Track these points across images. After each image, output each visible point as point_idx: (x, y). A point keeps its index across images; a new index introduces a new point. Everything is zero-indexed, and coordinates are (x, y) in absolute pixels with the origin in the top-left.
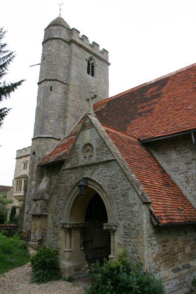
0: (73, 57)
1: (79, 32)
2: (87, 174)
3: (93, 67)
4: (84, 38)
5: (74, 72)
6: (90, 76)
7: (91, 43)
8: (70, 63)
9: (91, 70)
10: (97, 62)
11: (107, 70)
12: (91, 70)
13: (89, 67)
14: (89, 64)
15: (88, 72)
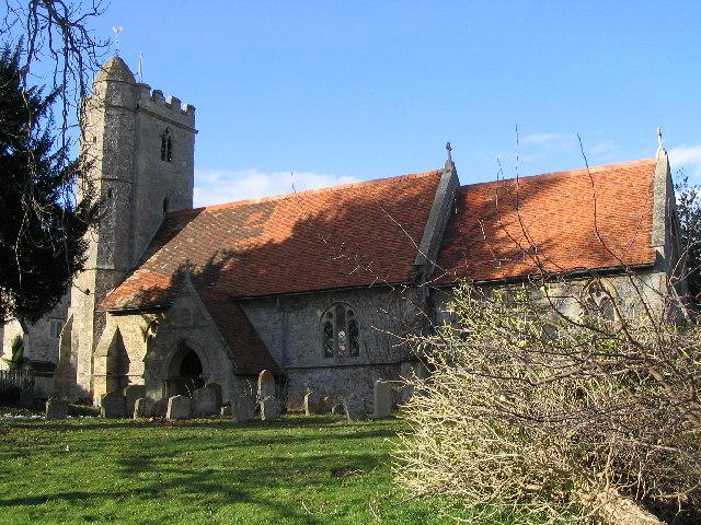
0: (142, 138)
1: (150, 89)
2: (185, 334)
3: (170, 144)
4: (158, 93)
5: (143, 163)
6: (164, 164)
7: (169, 101)
8: (136, 146)
9: (167, 151)
10: (175, 134)
11: (192, 142)
12: (167, 151)
13: (164, 146)
14: (163, 142)
15: (163, 158)
